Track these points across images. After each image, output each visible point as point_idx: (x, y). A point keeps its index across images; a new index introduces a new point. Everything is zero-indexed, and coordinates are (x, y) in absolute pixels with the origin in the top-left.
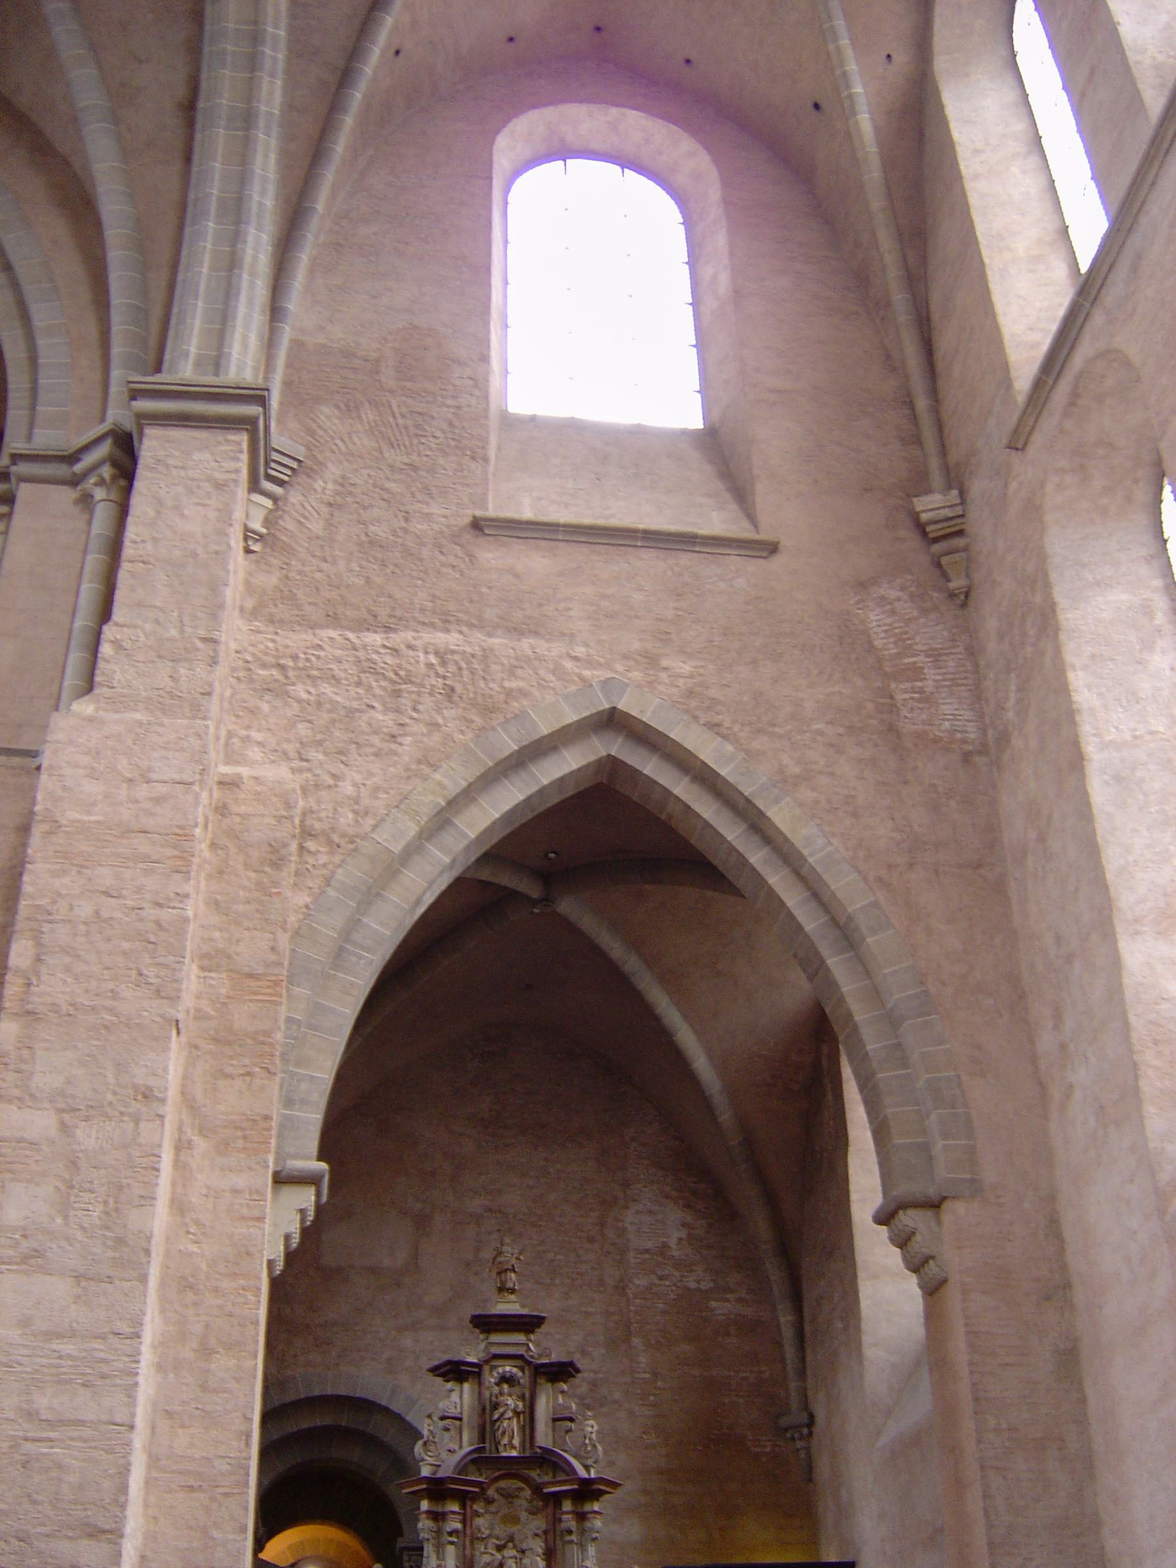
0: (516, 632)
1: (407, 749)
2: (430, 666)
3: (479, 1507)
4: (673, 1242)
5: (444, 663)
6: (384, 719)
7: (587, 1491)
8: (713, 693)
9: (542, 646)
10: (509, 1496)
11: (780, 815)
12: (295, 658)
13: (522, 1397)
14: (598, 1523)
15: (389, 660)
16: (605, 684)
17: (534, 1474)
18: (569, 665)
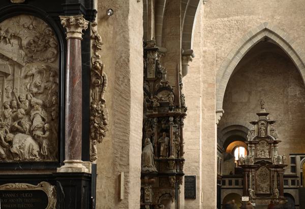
0: (250, 14)
1: (232, 41)
2: (235, 24)
3: (258, 145)
4: (297, 94)
5: (237, 23)
6: (228, 35)
7: (276, 142)
8: (283, 22)
9: (254, 16)
10: (263, 143)
11: (293, 46)
12: (213, 25)
13: (265, 127)
14: (277, 147)
15: (229, 23)
16: (264, 23)
17: (267, 139)
18: (258, 20)
